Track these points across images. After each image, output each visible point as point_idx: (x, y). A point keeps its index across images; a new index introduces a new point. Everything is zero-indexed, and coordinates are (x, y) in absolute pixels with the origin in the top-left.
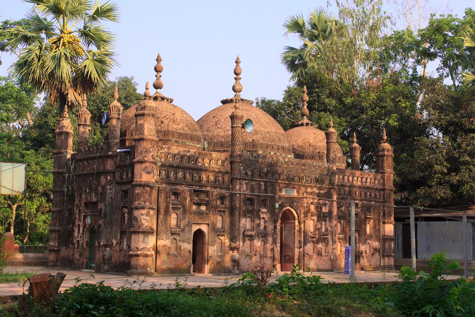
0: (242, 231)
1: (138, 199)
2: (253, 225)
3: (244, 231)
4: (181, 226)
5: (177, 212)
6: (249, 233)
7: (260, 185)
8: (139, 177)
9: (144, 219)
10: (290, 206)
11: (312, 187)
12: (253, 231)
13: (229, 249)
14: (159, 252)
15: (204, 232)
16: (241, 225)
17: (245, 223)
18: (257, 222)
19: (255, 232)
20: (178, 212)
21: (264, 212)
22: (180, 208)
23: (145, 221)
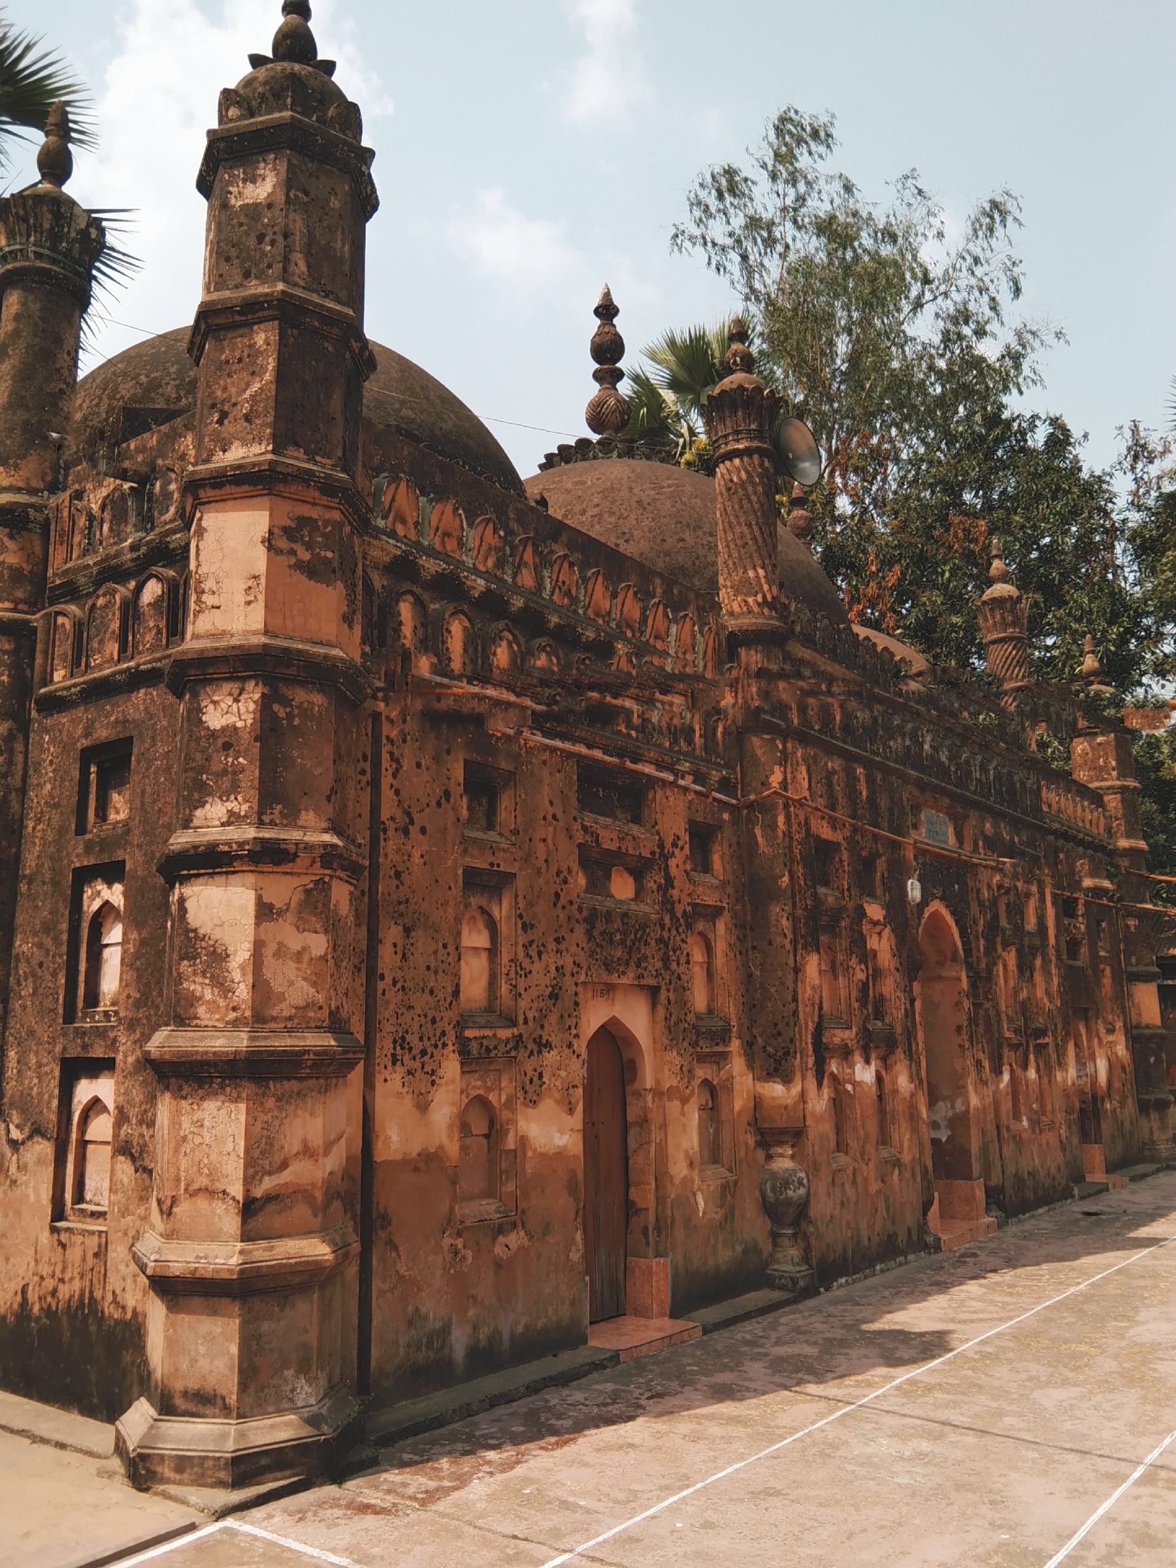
0: (811, 1026)
1: (226, 783)
2: (843, 993)
3: (819, 1030)
4: (523, 1004)
5: (496, 913)
6: (838, 1036)
7: (852, 779)
8: (241, 598)
9: (281, 952)
10: (942, 899)
11: (998, 815)
12: (849, 1028)
13: (751, 1140)
14: (386, 1220)
15: (629, 1040)
16: (806, 993)
17: (817, 982)
18: (861, 976)
19: (854, 1030)
20: (502, 911)
21: (876, 923)
22: (508, 878)
23: (290, 968)
